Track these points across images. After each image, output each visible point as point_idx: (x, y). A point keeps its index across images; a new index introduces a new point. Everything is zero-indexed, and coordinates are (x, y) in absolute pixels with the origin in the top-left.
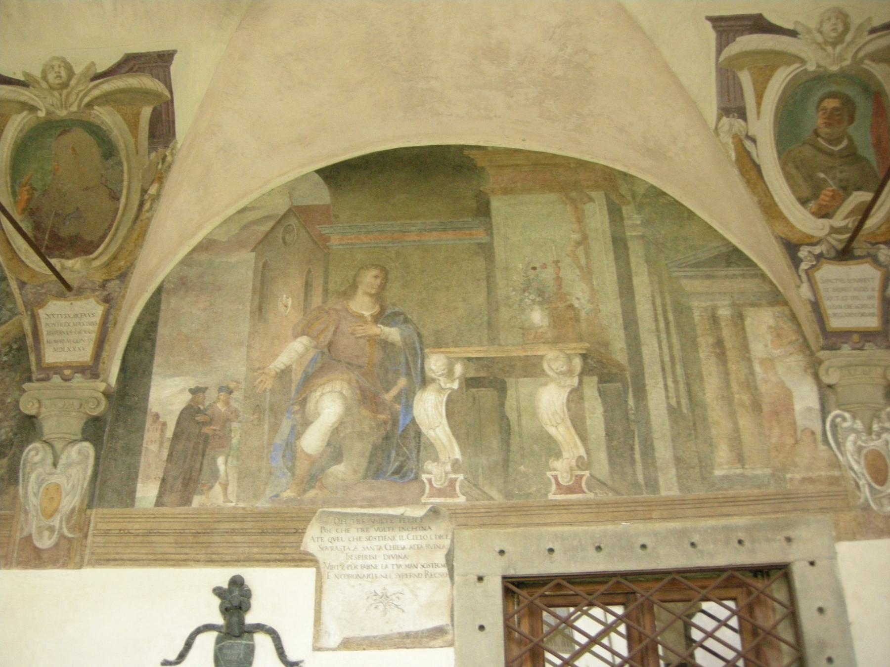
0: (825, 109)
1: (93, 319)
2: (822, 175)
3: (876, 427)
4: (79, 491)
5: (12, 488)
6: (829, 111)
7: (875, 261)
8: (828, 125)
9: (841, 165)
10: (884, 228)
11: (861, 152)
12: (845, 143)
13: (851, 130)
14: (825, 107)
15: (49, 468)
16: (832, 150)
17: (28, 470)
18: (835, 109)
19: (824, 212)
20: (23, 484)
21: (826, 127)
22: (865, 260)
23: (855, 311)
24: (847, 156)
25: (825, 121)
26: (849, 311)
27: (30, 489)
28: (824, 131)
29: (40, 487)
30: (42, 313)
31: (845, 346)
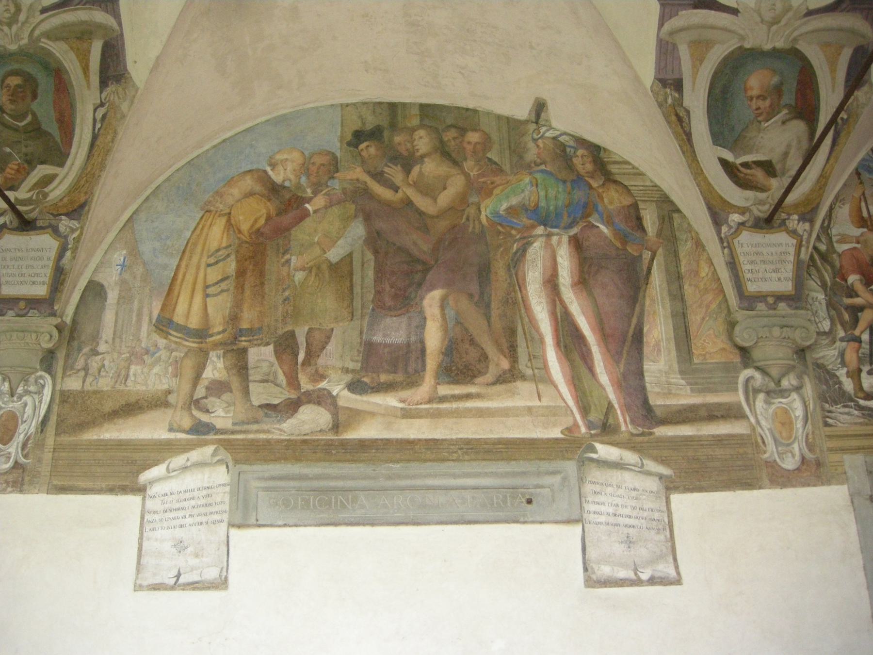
0: (8, 86)
2: (8, 150)
3: (20, 390)
6: (13, 87)
7: (55, 231)
8: (12, 101)
9: (26, 140)
10: (66, 200)
11: (44, 126)
12: (29, 118)
13: (34, 106)
14: (8, 84)
16: (17, 125)
18: (18, 86)
19: (9, 185)
21: (10, 103)
22: (46, 231)
23: (27, 279)
24: (30, 132)
25: (10, 98)
26: (22, 279)
28: (9, 107)
31: (11, 313)
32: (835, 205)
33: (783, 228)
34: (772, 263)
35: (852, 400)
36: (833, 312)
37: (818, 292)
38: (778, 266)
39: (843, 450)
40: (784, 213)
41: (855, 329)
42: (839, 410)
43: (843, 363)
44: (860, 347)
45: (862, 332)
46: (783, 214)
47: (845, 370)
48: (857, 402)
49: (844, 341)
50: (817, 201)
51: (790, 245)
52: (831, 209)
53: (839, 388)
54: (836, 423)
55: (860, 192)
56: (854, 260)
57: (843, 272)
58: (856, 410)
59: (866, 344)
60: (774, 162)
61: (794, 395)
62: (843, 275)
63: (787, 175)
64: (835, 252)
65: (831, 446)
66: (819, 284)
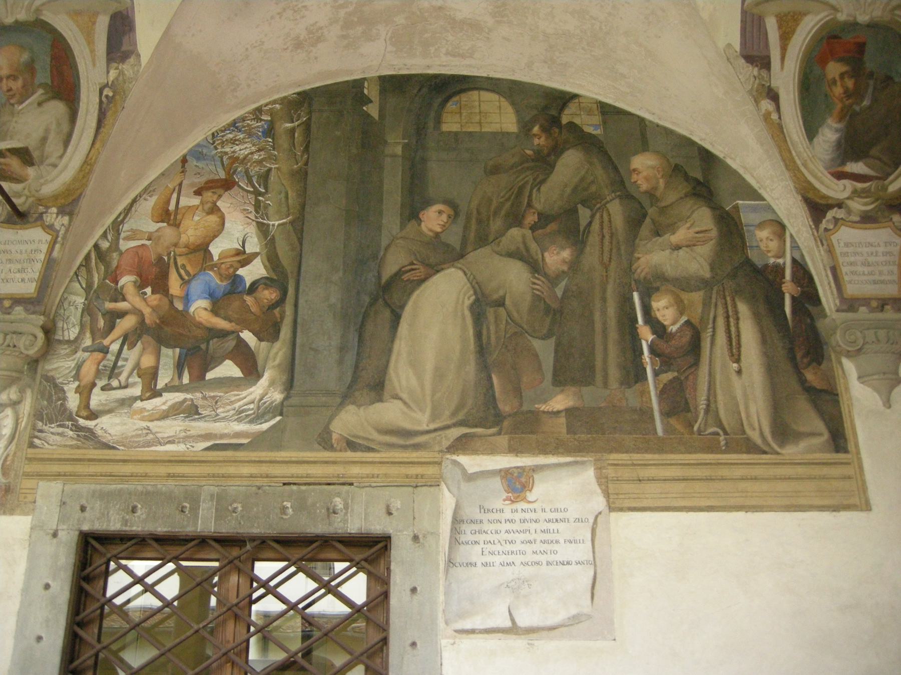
32: (140, 197)
33: (39, 223)
34: (19, 261)
35: (71, 418)
36: (87, 318)
37: (78, 295)
38: (25, 265)
39: (41, 476)
40: (42, 205)
41: (105, 338)
42: (52, 430)
43: (77, 377)
44: (103, 359)
45: (112, 343)
46: (41, 207)
47: (77, 383)
48: (77, 421)
49: (87, 352)
50: (79, 191)
51: (44, 241)
52: (134, 201)
53: (61, 404)
54: (43, 444)
55: (178, 182)
56: (136, 260)
57: (118, 272)
58: (71, 430)
59: (113, 355)
60: (31, 148)
61: (9, 411)
62: (116, 277)
63: (45, 163)
64: (117, 249)
65: (29, 470)
66: (84, 286)
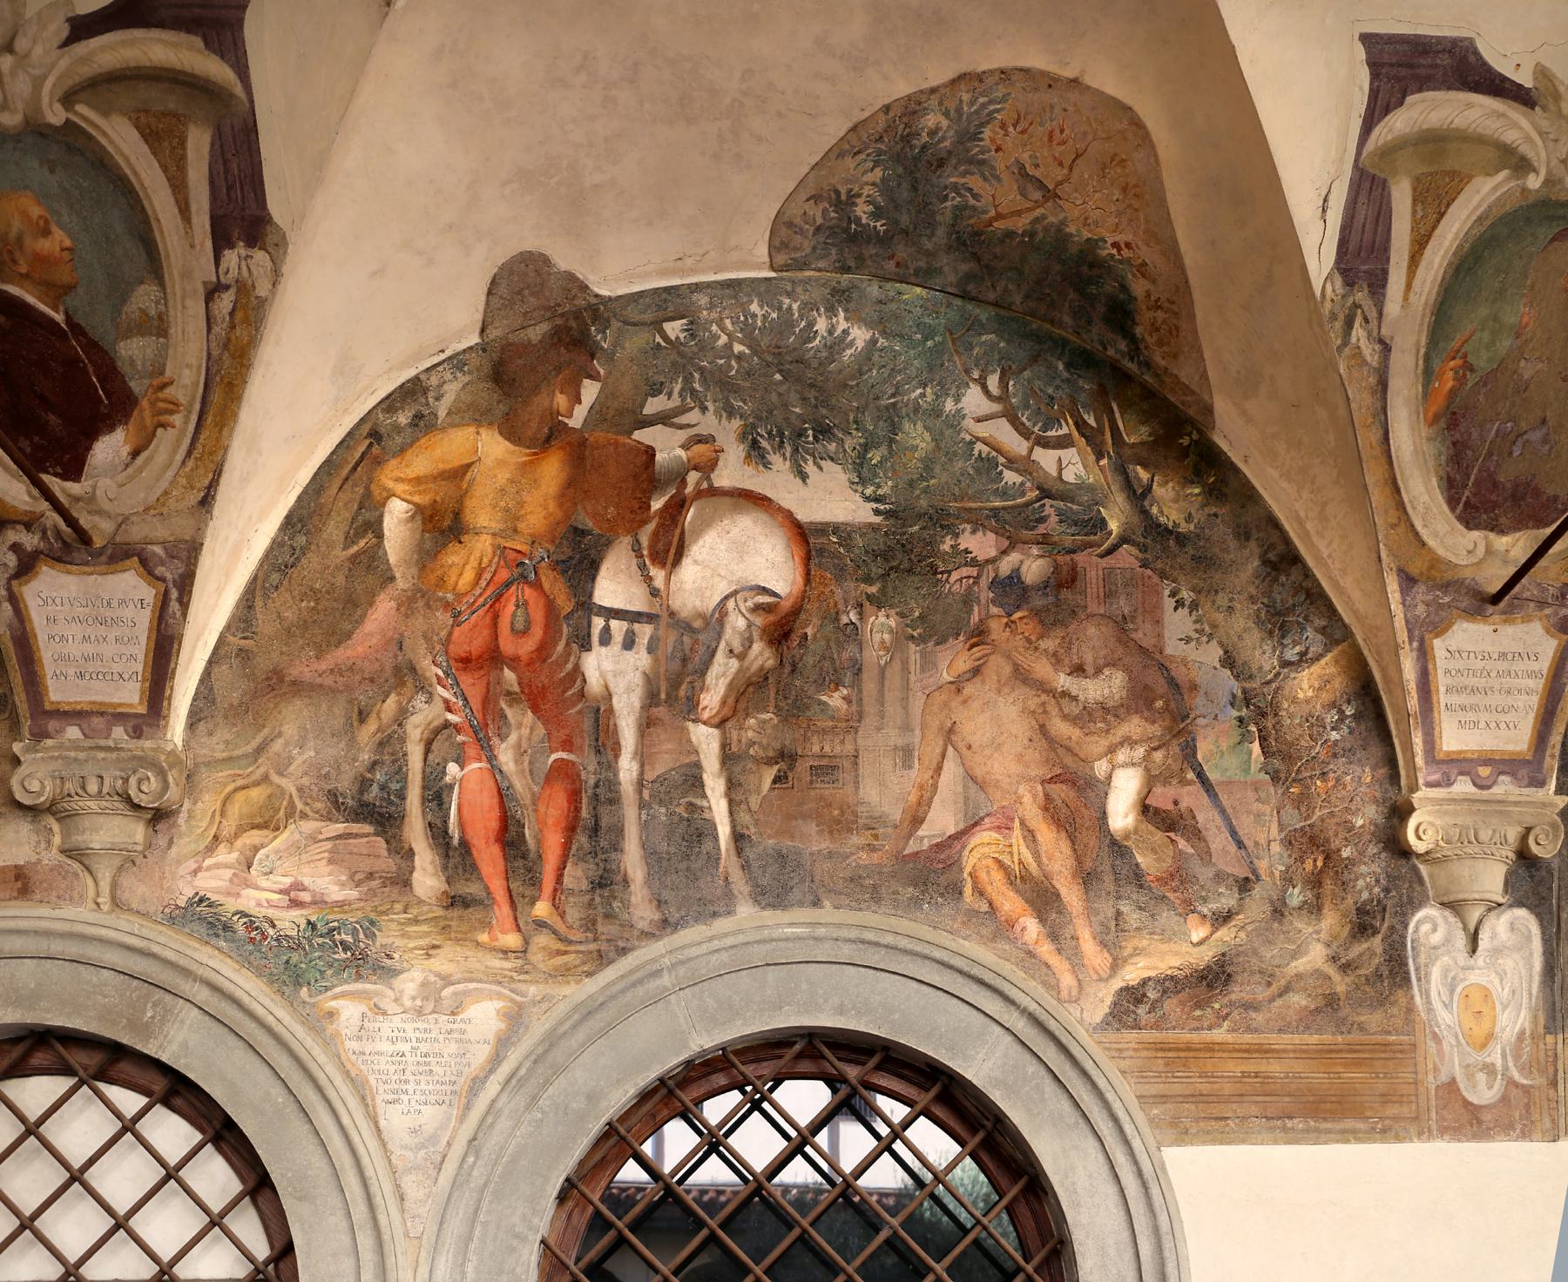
1: (1535, 666)
4: (1525, 1001)
5: (1400, 992)
15: (1462, 957)
17: (1422, 959)
20: (1419, 986)
27: (1434, 994)
29: (1452, 992)
30: (1439, 646)
